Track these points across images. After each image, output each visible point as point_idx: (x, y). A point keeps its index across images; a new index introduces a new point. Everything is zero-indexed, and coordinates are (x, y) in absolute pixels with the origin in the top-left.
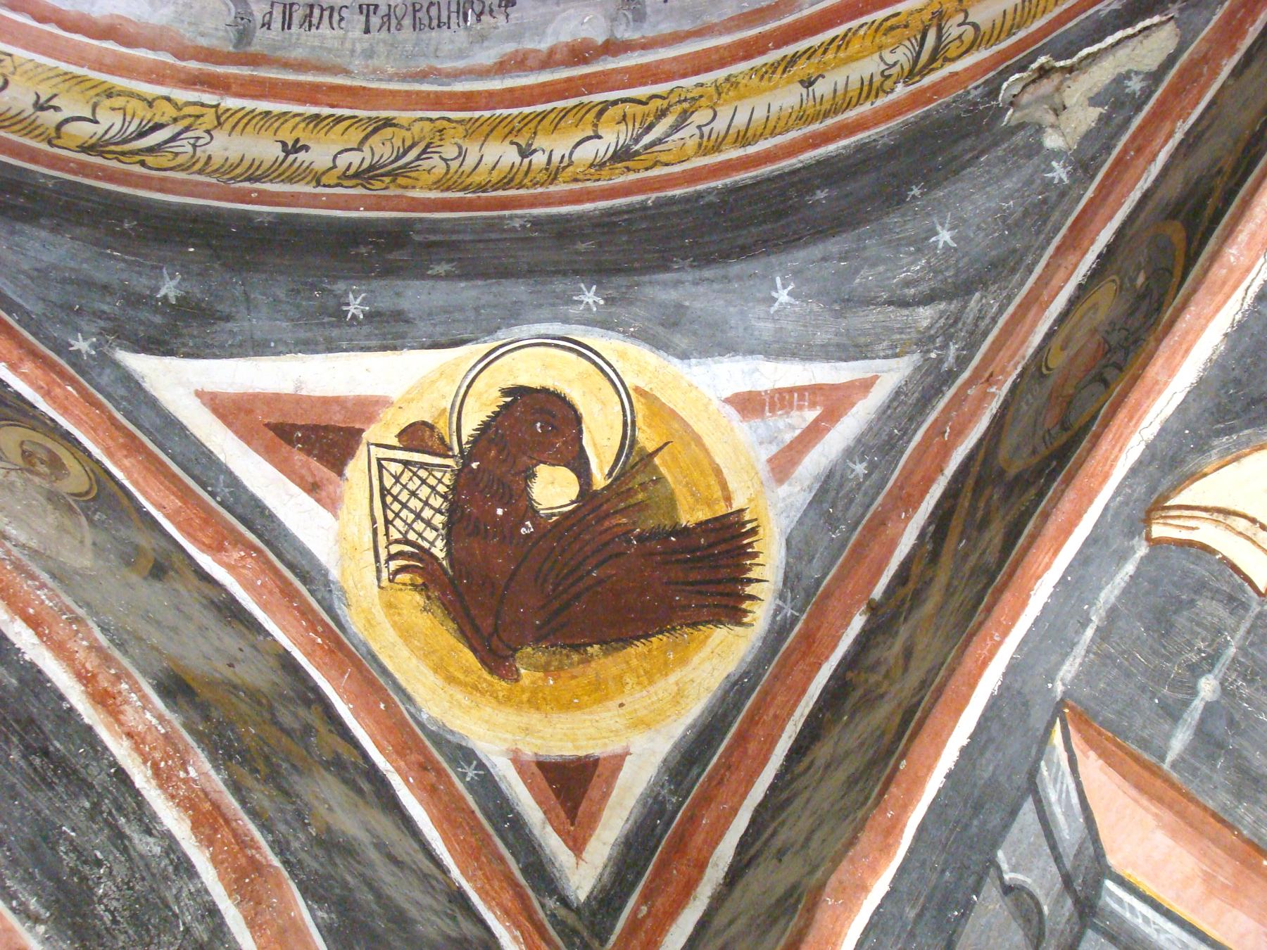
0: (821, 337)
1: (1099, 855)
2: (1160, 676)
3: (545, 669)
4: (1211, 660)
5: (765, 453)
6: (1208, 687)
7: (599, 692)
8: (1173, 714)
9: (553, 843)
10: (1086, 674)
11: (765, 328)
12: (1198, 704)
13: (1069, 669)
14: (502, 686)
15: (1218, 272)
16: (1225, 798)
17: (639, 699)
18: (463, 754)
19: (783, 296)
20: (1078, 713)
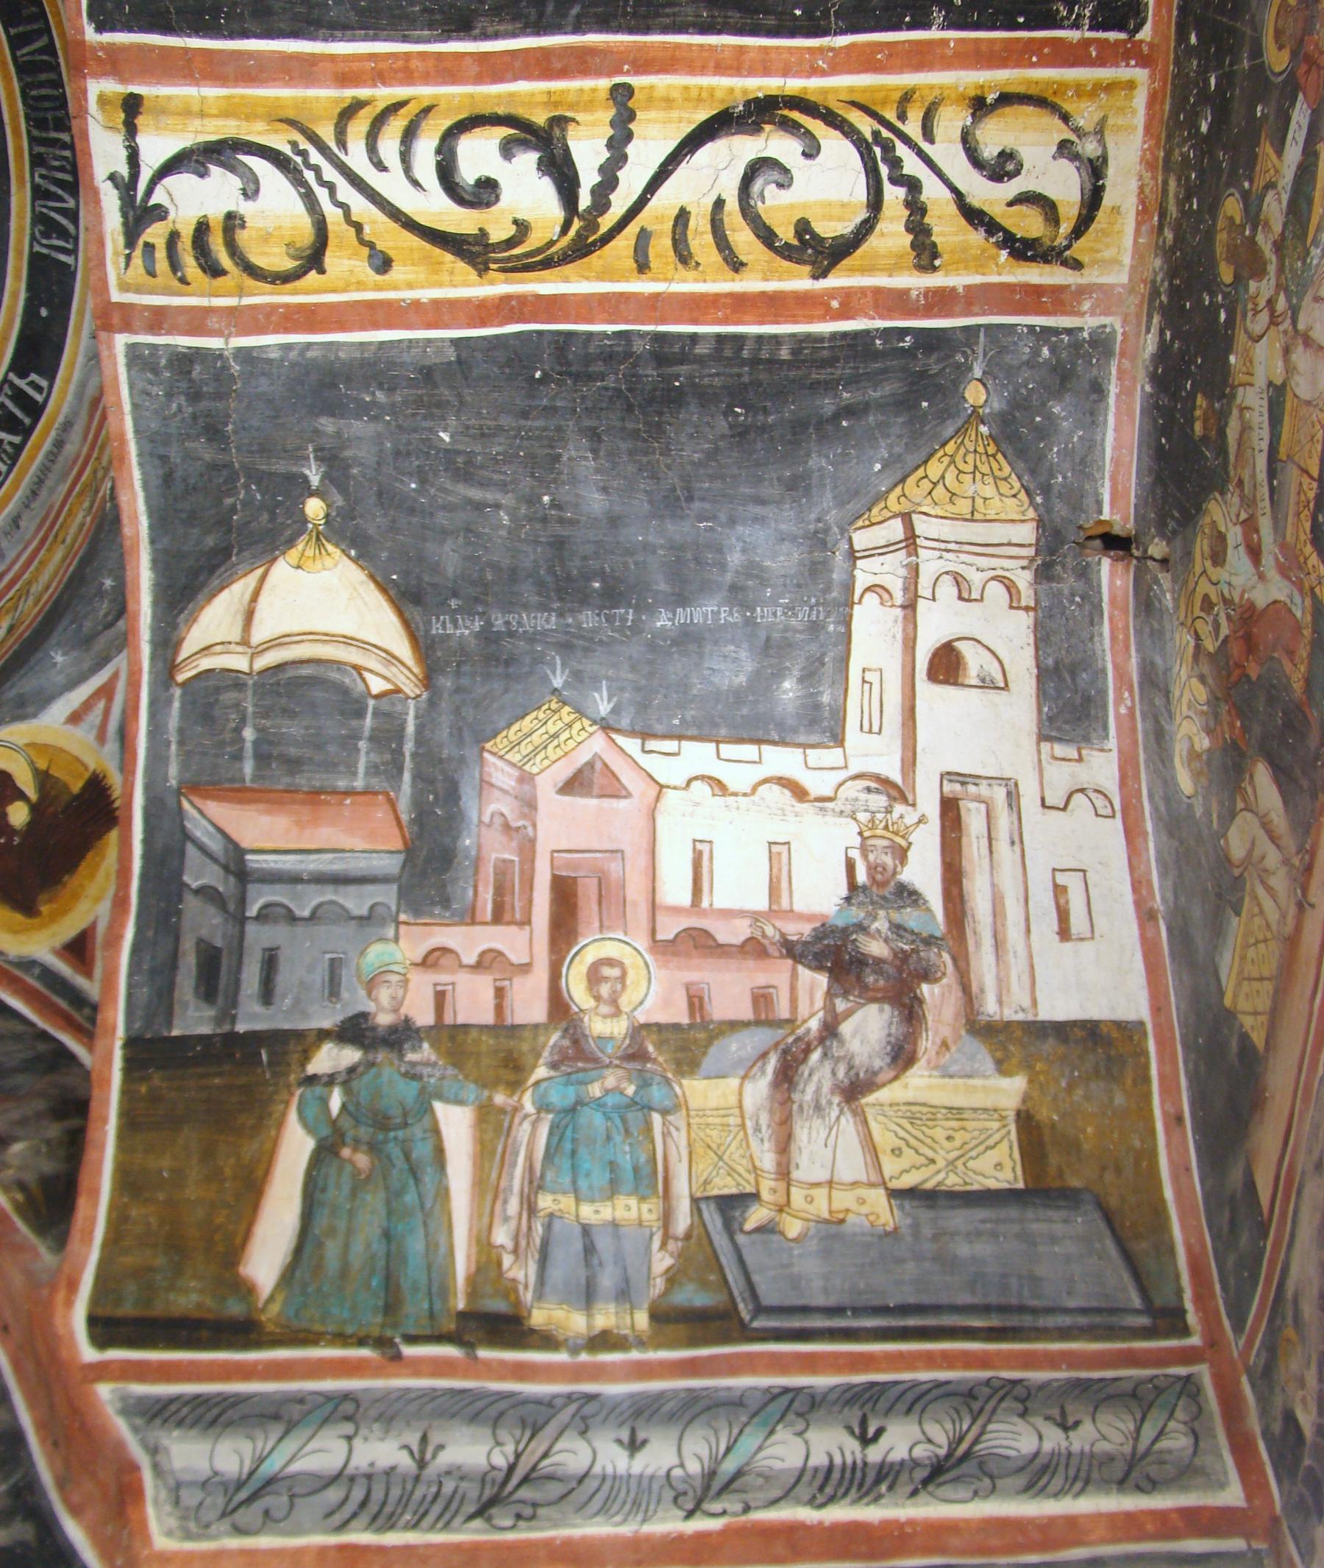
0: (86, 665)
1: (236, 846)
2: (222, 744)
3: (50, 901)
4: (243, 721)
5: (91, 737)
6: (249, 734)
7: (76, 897)
8: (238, 757)
9: (80, 981)
10: (184, 766)
11: (60, 679)
12: (249, 746)
13: (173, 770)
14: (35, 921)
15: (128, 543)
16: (287, 780)
17: (92, 889)
18: (28, 964)
19: (59, 659)
20: (193, 787)
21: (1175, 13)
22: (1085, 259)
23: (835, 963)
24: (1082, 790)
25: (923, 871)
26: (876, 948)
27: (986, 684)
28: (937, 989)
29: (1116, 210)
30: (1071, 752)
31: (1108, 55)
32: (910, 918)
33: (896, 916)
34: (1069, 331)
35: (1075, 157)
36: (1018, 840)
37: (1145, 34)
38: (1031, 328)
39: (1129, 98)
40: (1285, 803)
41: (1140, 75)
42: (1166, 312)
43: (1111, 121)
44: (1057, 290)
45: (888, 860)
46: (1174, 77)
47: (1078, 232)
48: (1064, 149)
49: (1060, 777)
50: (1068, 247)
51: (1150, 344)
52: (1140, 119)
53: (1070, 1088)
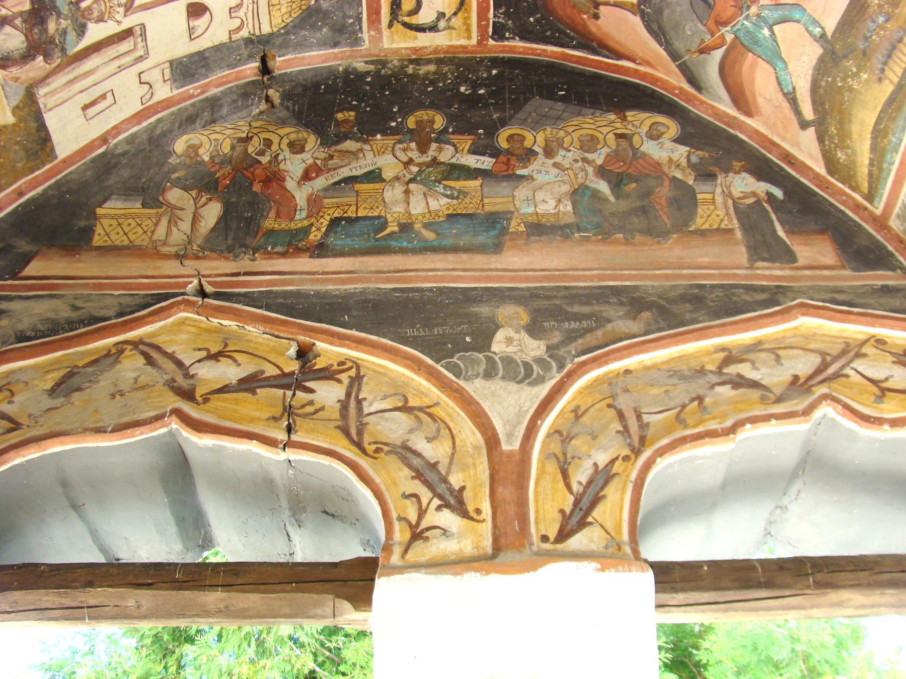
21: (501, 55)
22: (393, 29)
23: (38, 9)
24: (151, 87)
25: (95, 32)
26: (52, 27)
27: (191, 30)
28: (42, 64)
29: (416, 38)
30: (168, 75)
31: (482, 29)
32: (71, 36)
33: (70, 29)
34: (361, 28)
35: (438, 19)
36: (121, 69)
37: (491, 42)
38: (361, 13)
39: (464, 38)
40: (213, 229)
41: (474, 41)
42: (377, 75)
43: (454, 31)
44: (379, 21)
45: (96, 14)
46: (475, 58)
47: (405, 25)
48: (442, 15)
49: (154, 76)
50: (398, 22)
51: (361, 66)
52: (455, 43)
53: (17, 143)
